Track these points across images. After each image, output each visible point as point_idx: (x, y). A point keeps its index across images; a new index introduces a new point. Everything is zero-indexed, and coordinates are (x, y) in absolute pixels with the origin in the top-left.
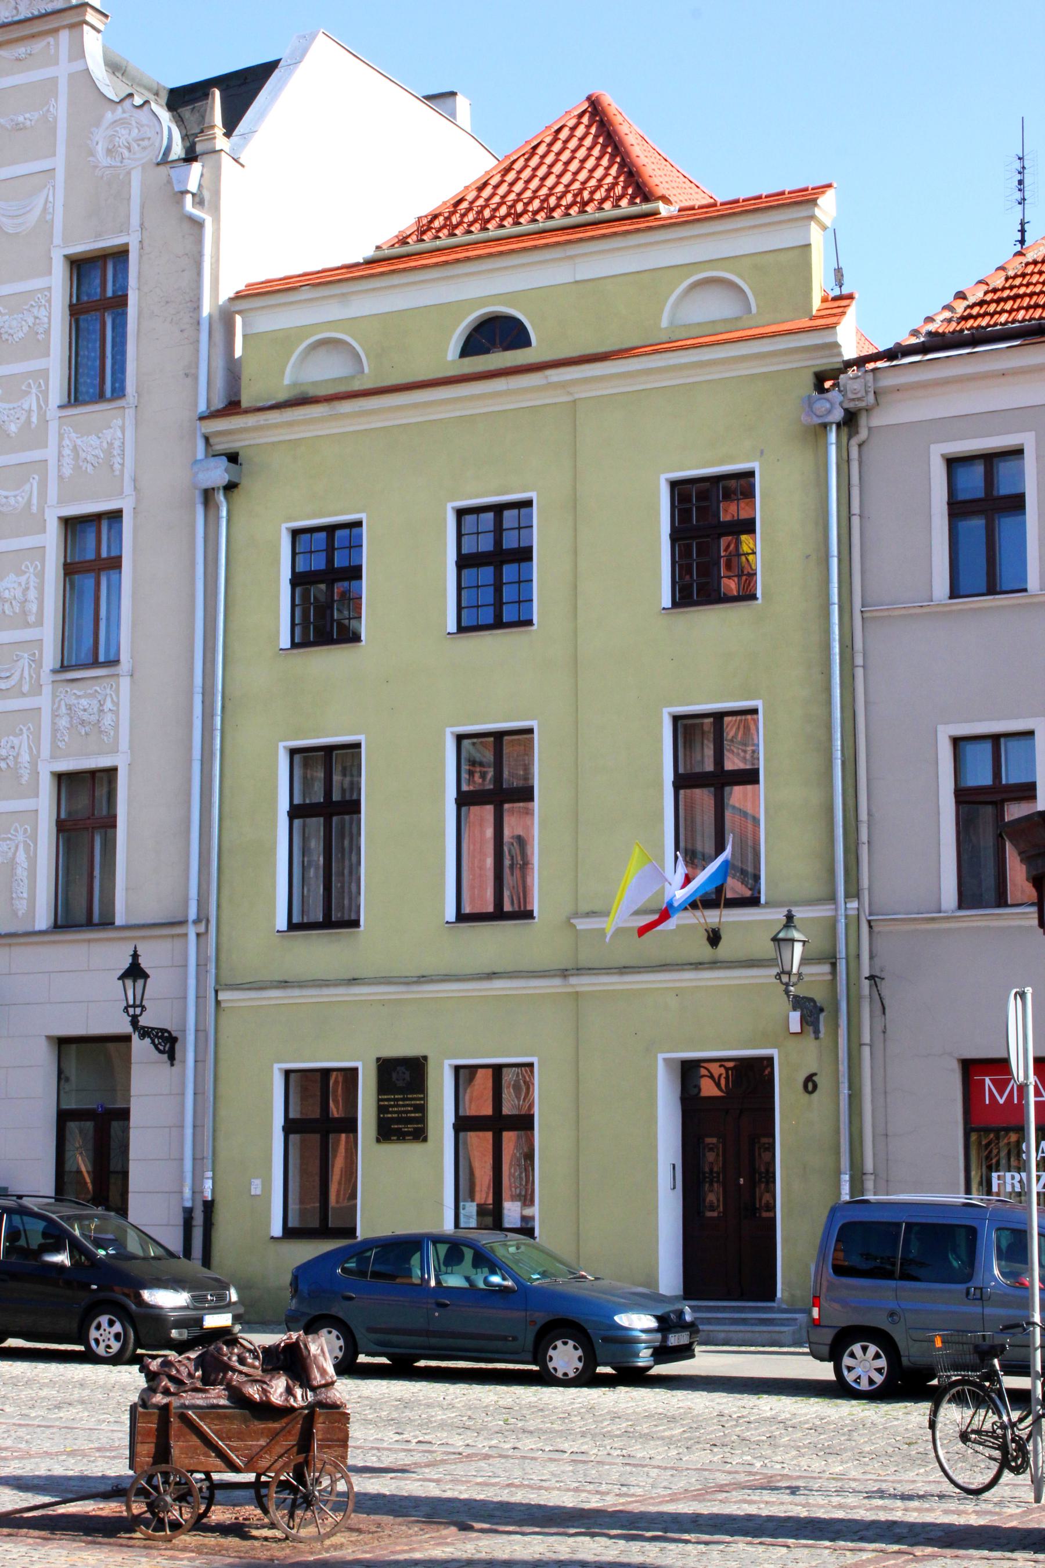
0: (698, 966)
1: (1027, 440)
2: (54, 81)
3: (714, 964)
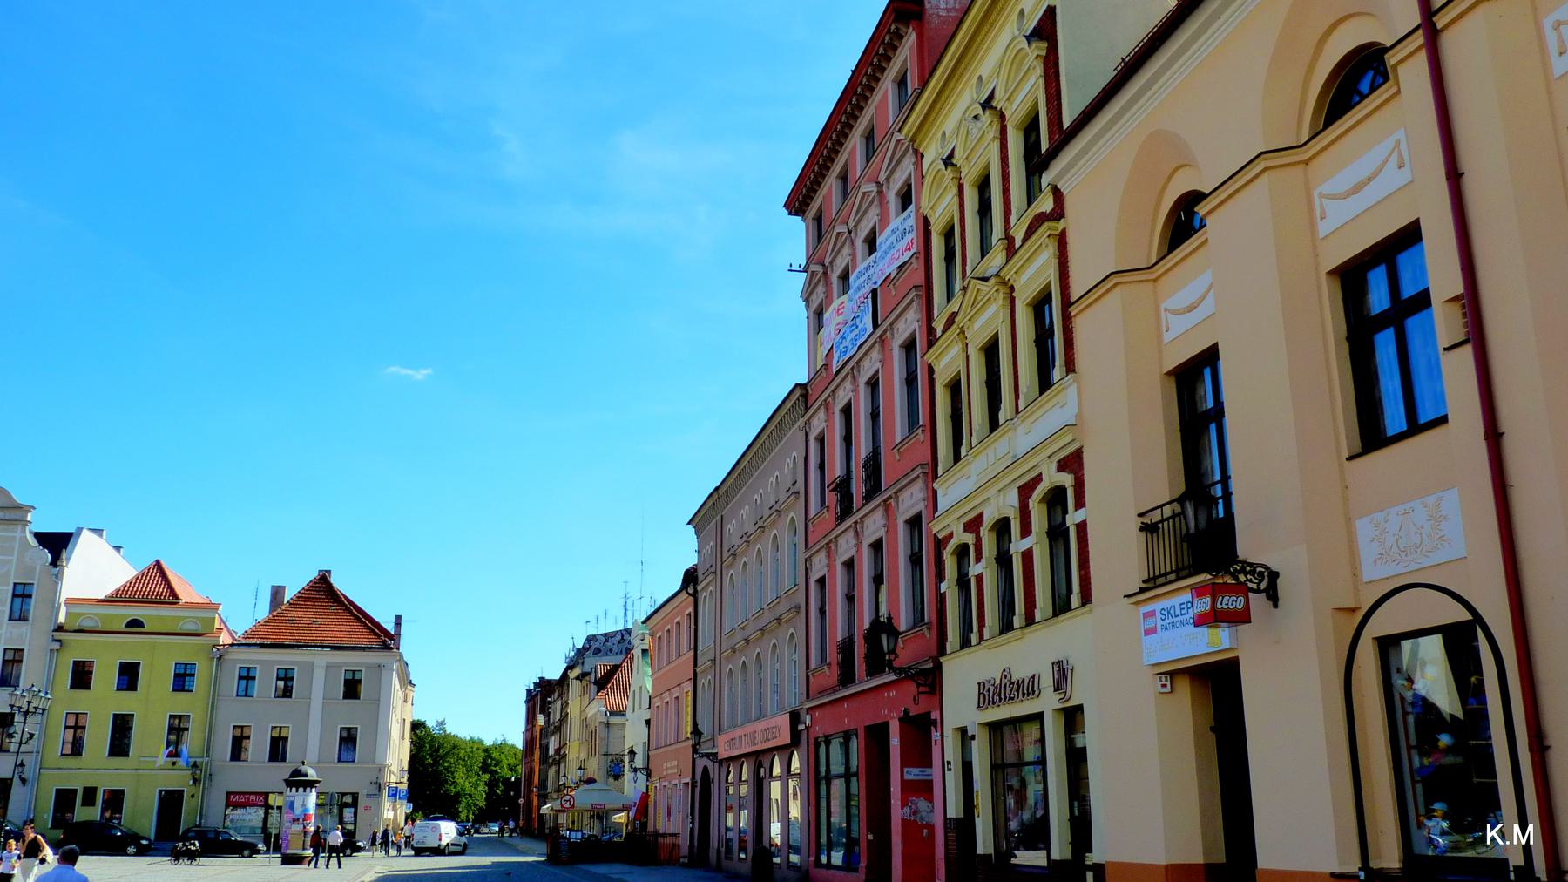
0: (169, 770)
2: (14, 537)
3: (174, 770)
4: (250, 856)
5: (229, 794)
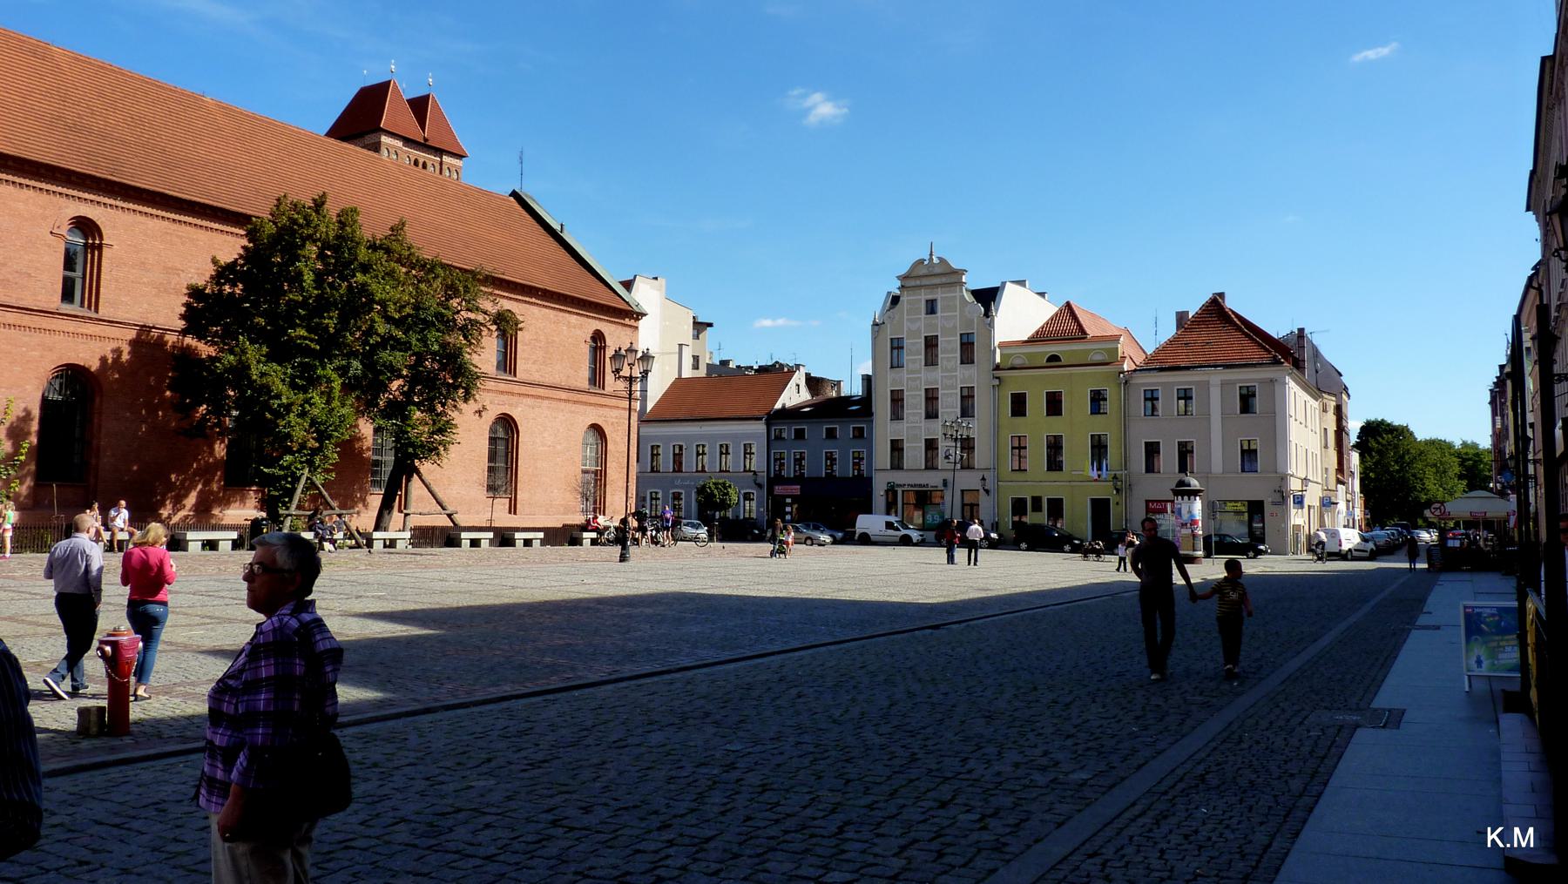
1: (1160, 388)
2: (955, 296)
3: (1099, 481)
4: (1255, 557)
5: (1147, 502)
